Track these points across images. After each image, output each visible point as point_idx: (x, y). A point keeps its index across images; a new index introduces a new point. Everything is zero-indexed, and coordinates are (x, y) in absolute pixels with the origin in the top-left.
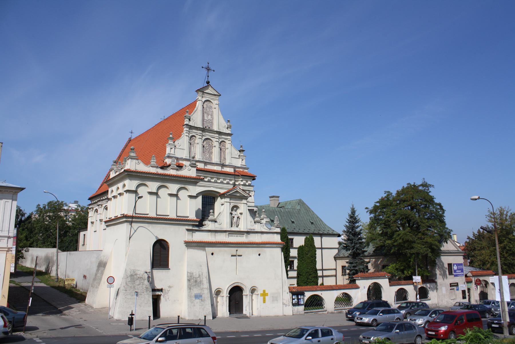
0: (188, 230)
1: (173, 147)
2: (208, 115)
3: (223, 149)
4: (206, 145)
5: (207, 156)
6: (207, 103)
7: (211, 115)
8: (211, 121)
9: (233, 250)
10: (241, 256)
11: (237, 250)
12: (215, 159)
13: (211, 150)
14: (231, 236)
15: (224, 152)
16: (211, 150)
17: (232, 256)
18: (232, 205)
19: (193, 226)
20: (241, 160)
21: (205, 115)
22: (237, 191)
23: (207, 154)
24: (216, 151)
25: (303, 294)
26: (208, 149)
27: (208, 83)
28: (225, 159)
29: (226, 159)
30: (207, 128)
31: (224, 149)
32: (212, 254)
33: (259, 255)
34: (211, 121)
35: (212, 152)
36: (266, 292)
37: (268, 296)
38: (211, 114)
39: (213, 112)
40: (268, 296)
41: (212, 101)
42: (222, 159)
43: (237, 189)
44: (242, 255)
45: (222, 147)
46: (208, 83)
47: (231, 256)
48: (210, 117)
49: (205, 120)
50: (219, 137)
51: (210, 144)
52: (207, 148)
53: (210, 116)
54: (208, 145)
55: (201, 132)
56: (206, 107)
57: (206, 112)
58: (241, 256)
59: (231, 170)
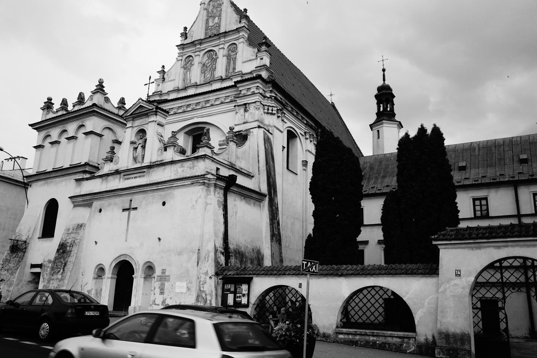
0: (77, 180)
1: (160, 83)
2: (215, 18)
4: (207, 61)
5: (208, 76)
7: (218, 16)
8: (218, 25)
9: (123, 201)
10: (136, 209)
11: (131, 200)
13: (214, 66)
14: (128, 179)
15: (235, 59)
16: (214, 66)
17: (124, 210)
18: (136, 130)
19: (85, 172)
20: (259, 59)
22: (141, 105)
23: (208, 73)
25: (248, 281)
26: (210, 65)
31: (234, 55)
32: (100, 211)
33: (164, 204)
36: (167, 274)
37: (169, 281)
38: (219, 15)
40: (169, 281)
42: (231, 70)
43: (140, 103)
44: (136, 208)
47: (123, 211)
48: (217, 18)
50: (224, 41)
52: (208, 66)
53: (217, 18)
54: (210, 61)
55: (198, 46)
57: (211, 17)
58: (136, 209)
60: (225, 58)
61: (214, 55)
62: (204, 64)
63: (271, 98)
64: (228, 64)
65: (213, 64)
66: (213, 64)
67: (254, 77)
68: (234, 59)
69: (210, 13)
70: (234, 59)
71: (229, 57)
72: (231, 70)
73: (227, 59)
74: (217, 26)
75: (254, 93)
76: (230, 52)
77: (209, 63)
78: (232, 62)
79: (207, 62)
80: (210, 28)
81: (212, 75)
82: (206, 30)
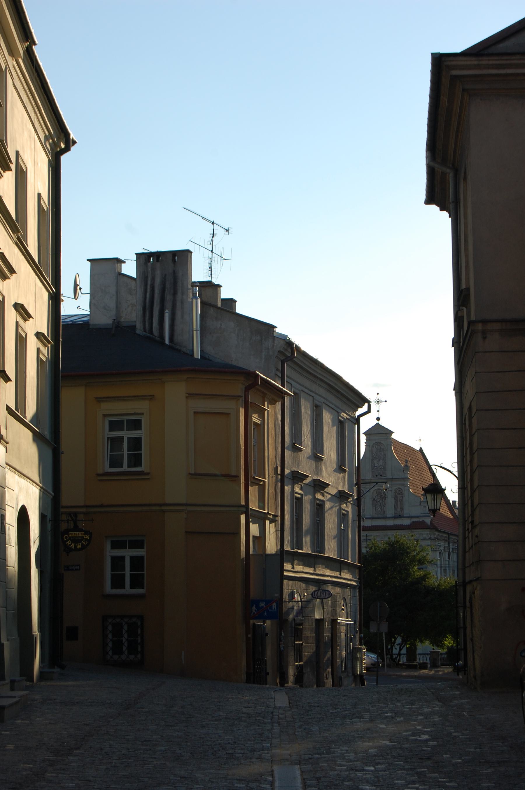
3: (399, 498)
4: (377, 497)
5: (379, 509)
6: (376, 446)
8: (383, 467)
12: (390, 511)
13: (383, 502)
16: (383, 502)
20: (422, 507)
21: (375, 462)
24: (390, 502)
26: (380, 501)
27: (378, 419)
28: (402, 509)
29: (403, 510)
30: (378, 476)
31: (400, 497)
34: (383, 467)
35: (384, 503)
39: (385, 455)
41: (382, 442)
42: (399, 509)
45: (398, 496)
46: (378, 419)
48: (381, 461)
49: (375, 468)
51: (382, 495)
52: (378, 501)
53: (381, 461)
54: (379, 497)
56: (376, 452)
57: (376, 458)
59: (407, 522)
60: (393, 499)
61: (383, 493)
62: (374, 499)
63: (435, 540)
64: (396, 503)
65: (383, 501)
66: (383, 501)
67: (420, 521)
68: (400, 501)
69: (375, 454)
70: (400, 501)
71: (396, 498)
72: (399, 509)
73: (395, 499)
74: (382, 468)
75: (424, 539)
76: (397, 494)
77: (378, 499)
78: (399, 503)
79: (377, 498)
80: (375, 468)
81: (383, 510)
82: (372, 469)
